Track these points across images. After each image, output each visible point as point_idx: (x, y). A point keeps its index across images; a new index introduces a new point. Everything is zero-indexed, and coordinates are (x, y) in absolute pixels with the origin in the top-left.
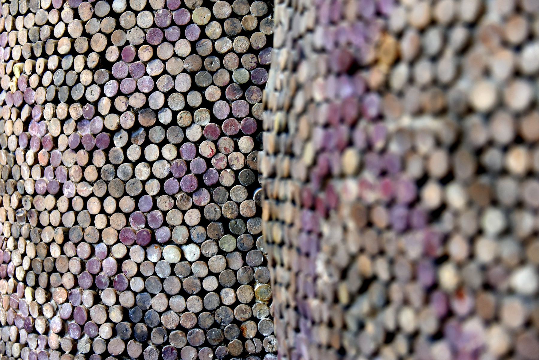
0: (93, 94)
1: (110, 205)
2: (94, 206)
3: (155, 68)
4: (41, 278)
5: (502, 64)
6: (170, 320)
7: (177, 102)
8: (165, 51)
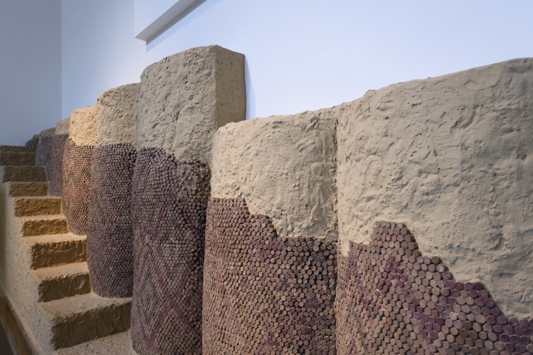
0: (112, 192)
1: (114, 210)
2: (112, 210)
3: (122, 189)
4: (103, 222)
6: (124, 228)
7: (125, 194)
8: (124, 186)
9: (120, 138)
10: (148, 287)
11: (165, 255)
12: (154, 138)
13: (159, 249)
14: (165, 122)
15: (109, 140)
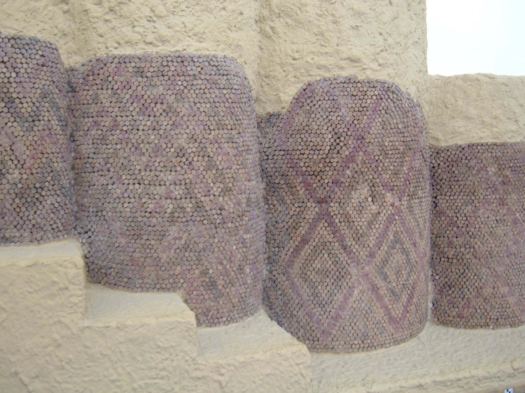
0: (238, 141)
2: (240, 171)
5: (388, 140)
10: (398, 258)
12: (379, 68)
13: (410, 208)
15: (199, 45)
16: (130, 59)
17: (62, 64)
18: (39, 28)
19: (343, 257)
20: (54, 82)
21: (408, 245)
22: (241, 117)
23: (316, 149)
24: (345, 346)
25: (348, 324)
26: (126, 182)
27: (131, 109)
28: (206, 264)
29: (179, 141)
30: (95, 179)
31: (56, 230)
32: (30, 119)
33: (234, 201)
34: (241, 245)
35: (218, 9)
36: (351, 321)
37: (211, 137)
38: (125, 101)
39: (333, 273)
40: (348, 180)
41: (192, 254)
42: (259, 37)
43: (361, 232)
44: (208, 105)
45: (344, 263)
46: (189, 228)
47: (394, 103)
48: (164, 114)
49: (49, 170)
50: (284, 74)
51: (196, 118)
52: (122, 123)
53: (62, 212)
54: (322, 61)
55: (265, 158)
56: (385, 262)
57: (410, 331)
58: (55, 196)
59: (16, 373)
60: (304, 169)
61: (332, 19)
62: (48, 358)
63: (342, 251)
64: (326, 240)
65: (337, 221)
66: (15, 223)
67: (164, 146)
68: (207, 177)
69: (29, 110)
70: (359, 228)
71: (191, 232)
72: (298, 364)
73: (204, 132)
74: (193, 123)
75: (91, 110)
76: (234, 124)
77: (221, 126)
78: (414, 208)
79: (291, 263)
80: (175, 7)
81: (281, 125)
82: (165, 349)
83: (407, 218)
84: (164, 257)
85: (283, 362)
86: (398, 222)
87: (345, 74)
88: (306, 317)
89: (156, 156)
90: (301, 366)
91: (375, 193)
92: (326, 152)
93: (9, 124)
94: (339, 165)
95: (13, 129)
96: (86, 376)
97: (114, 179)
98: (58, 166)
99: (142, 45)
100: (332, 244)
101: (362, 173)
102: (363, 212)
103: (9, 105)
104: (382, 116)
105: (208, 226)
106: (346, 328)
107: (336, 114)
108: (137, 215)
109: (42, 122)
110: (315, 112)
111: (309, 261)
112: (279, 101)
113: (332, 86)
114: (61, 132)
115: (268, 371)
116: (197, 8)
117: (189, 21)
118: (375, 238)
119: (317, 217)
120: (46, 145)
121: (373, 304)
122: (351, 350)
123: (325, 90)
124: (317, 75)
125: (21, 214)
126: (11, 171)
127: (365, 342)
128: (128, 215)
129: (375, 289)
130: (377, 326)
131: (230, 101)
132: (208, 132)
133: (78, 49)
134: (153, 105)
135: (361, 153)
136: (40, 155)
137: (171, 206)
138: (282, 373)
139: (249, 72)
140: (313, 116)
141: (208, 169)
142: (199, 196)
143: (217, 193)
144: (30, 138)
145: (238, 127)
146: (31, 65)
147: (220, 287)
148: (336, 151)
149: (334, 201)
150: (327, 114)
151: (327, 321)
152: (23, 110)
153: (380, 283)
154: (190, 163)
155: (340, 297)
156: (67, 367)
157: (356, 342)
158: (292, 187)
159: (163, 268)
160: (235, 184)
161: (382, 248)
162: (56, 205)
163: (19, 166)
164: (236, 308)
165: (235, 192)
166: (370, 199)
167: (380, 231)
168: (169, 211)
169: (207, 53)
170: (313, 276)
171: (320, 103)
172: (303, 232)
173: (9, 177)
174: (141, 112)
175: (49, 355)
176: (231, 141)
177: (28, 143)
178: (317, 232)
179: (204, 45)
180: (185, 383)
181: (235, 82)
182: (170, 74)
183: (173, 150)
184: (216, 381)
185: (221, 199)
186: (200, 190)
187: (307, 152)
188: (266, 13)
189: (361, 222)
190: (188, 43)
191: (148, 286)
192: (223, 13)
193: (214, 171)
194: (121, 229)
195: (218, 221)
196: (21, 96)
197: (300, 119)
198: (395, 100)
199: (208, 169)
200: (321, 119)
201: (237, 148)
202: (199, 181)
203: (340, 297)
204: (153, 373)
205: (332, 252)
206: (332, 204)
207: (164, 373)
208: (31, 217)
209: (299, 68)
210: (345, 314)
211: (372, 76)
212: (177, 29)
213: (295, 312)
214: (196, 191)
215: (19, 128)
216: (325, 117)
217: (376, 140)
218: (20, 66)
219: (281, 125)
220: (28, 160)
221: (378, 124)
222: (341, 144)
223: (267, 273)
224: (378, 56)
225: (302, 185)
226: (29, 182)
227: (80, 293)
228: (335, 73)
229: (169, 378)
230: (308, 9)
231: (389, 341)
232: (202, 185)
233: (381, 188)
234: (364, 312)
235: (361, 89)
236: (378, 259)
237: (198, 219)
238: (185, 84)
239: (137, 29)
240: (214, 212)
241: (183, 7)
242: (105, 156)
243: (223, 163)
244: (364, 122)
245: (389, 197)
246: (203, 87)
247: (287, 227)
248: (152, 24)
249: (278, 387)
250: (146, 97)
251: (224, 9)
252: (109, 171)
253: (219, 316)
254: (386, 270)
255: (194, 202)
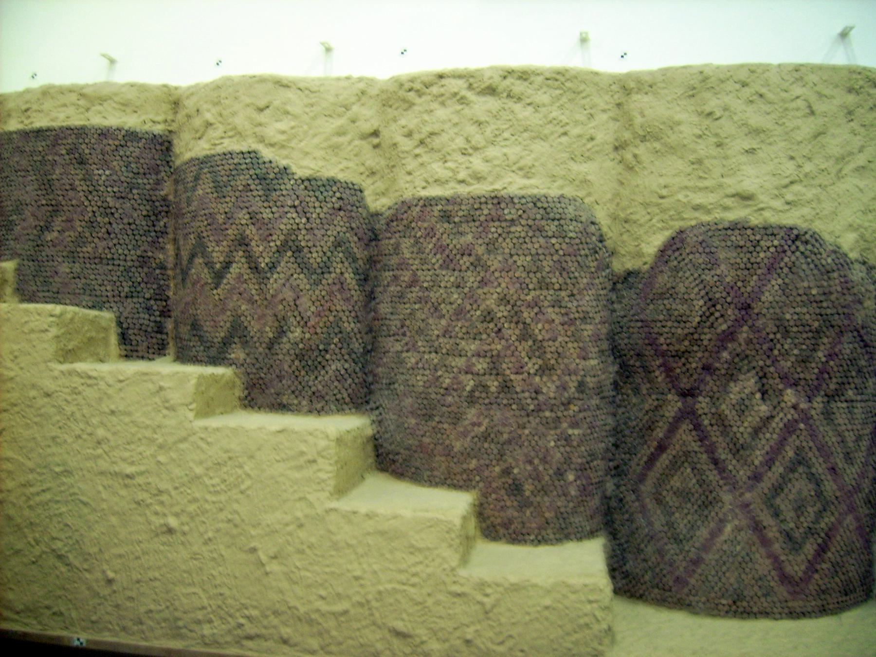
0: (569, 305)
2: (570, 345)
5: (792, 311)
9: (560, 182)
10: (800, 486)
11: (841, 421)
13: (828, 415)
14: (817, 182)
15: (527, 182)
16: (436, 200)
17: (366, 207)
18: (341, 166)
19: (712, 476)
20: (352, 229)
21: (819, 468)
22: (577, 274)
23: (681, 320)
24: (708, 605)
25: (713, 573)
26: (422, 349)
27: (434, 261)
28: (510, 460)
29: (488, 302)
30: (390, 344)
31: (341, 401)
32: (319, 271)
33: (558, 383)
34: (563, 442)
35: (556, 135)
36: (717, 568)
37: (529, 298)
38: (427, 251)
39: (696, 495)
40: (726, 366)
41: (493, 446)
42: (620, 168)
43: (741, 441)
44: (529, 258)
45: (714, 483)
46: (492, 412)
47: (806, 257)
48: (471, 268)
49: (337, 330)
50: (648, 217)
51: (511, 274)
52: (422, 278)
53: (349, 381)
54: (698, 199)
55: (619, 330)
56: (778, 489)
57: (819, 603)
58: (342, 361)
59: (254, 550)
60: (665, 347)
61: (715, 140)
62: (289, 538)
63: (712, 467)
64: (690, 449)
65: (706, 422)
66: (293, 388)
67: (468, 307)
68: (520, 348)
69: (319, 260)
70: (738, 435)
71: (495, 419)
72: (590, 602)
73: (520, 292)
74: (507, 279)
75: (392, 262)
76: (566, 283)
77: (544, 285)
78: (838, 415)
79: (642, 478)
80: (496, 136)
81: (640, 286)
82: (420, 550)
83: (821, 429)
84: (458, 446)
85: (569, 595)
86: (804, 433)
87: (731, 216)
88: (657, 556)
89: (458, 320)
90: (595, 605)
91: (767, 387)
92: (695, 324)
93: (295, 276)
94: (713, 343)
95: (299, 282)
96: (328, 566)
97: (410, 346)
98: (349, 326)
99: (452, 184)
100: (699, 455)
101: (747, 356)
102: (746, 413)
103: (296, 255)
104: (782, 275)
105: (517, 413)
106: (710, 578)
107: (713, 272)
108: (430, 390)
109: (333, 275)
110: (685, 268)
111: (666, 475)
112: (639, 254)
113: (710, 234)
114: (357, 287)
115: (547, 602)
116: (525, 135)
117: (513, 152)
118: (763, 452)
119: (679, 415)
120: (335, 301)
121: (754, 548)
122: (716, 612)
123: (701, 238)
124: (692, 219)
125: (300, 379)
126: (292, 328)
127: (739, 603)
128: (421, 389)
129: (758, 528)
130: (760, 583)
131: (561, 253)
132: (526, 291)
133: (387, 190)
134: (458, 257)
135: (745, 328)
136: (327, 313)
137: (472, 383)
138: (567, 608)
139: (601, 216)
140: (680, 274)
141: (522, 338)
142: (508, 372)
143: (532, 371)
144: (317, 292)
145: (570, 287)
146: (325, 209)
147: (527, 493)
148: (708, 324)
149: (704, 393)
150: (700, 271)
151: (684, 564)
152: (311, 261)
153: (767, 519)
154: (500, 330)
155: (703, 533)
156: (308, 551)
157: (724, 602)
158: (648, 371)
159: (455, 460)
160: (560, 360)
161: (774, 469)
162: (343, 372)
163: (302, 323)
164: (552, 525)
165: (559, 372)
166: (758, 396)
167: (772, 443)
168: (468, 388)
169: (535, 191)
170: (670, 499)
171: (691, 256)
172: (661, 435)
173: (291, 335)
174: (445, 266)
175: (290, 534)
176: (557, 303)
177: (314, 298)
178: (678, 436)
179: (532, 181)
180: (441, 597)
181: (571, 228)
182: (482, 218)
183: (478, 313)
184: (479, 602)
185: (537, 379)
186: (510, 365)
187: (669, 324)
188: (627, 135)
189: (743, 429)
190: (510, 180)
191: (437, 480)
192: (564, 139)
193: (530, 343)
194: (412, 406)
195: (532, 407)
196: (310, 244)
197: (663, 280)
198: (807, 253)
199: (522, 338)
200: (691, 279)
201: (567, 314)
202: (509, 353)
203: (703, 533)
204: (403, 577)
205: (698, 466)
206: (700, 399)
207: (415, 580)
208: (311, 383)
209: (669, 210)
210: (710, 557)
211: (771, 218)
212: (496, 162)
213: (642, 546)
214: (504, 366)
215: (305, 281)
216: (696, 275)
217: (771, 311)
218: (312, 210)
219: (640, 286)
220: (312, 318)
221: (777, 287)
222: (717, 314)
223: (614, 487)
224: (785, 190)
225: (662, 369)
226: (312, 343)
227: (330, 468)
228: (717, 216)
229: (422, 587)
230: (682, 128)
231: (780, 610)
232: (513, 359)
233: (778, 380)
234: (740, 559)
235: (752, 238)
236: (766, 485)
237: (505, 402)
238: (500, 231)
239: (449, 164)
240: (527, 394)
241: (506, 135)
242: (402, 317)
243: (543, 332)
244: (752, 283)
245: (790, 396)
246: (523, 234)
247: (641, 425)
248: (466, 158)
249: (560, 626)
250: (451, 246)
251: (565, 134)
252: (404, 334)
253: (524, 531)
254: (778, 501)
255: (500, 380)
